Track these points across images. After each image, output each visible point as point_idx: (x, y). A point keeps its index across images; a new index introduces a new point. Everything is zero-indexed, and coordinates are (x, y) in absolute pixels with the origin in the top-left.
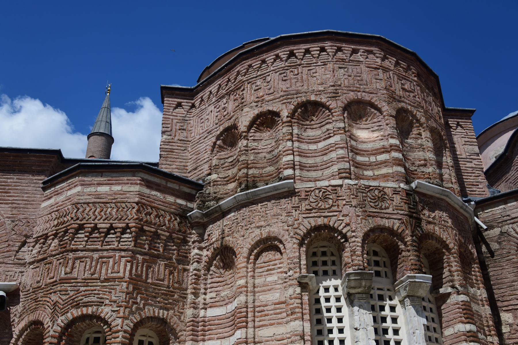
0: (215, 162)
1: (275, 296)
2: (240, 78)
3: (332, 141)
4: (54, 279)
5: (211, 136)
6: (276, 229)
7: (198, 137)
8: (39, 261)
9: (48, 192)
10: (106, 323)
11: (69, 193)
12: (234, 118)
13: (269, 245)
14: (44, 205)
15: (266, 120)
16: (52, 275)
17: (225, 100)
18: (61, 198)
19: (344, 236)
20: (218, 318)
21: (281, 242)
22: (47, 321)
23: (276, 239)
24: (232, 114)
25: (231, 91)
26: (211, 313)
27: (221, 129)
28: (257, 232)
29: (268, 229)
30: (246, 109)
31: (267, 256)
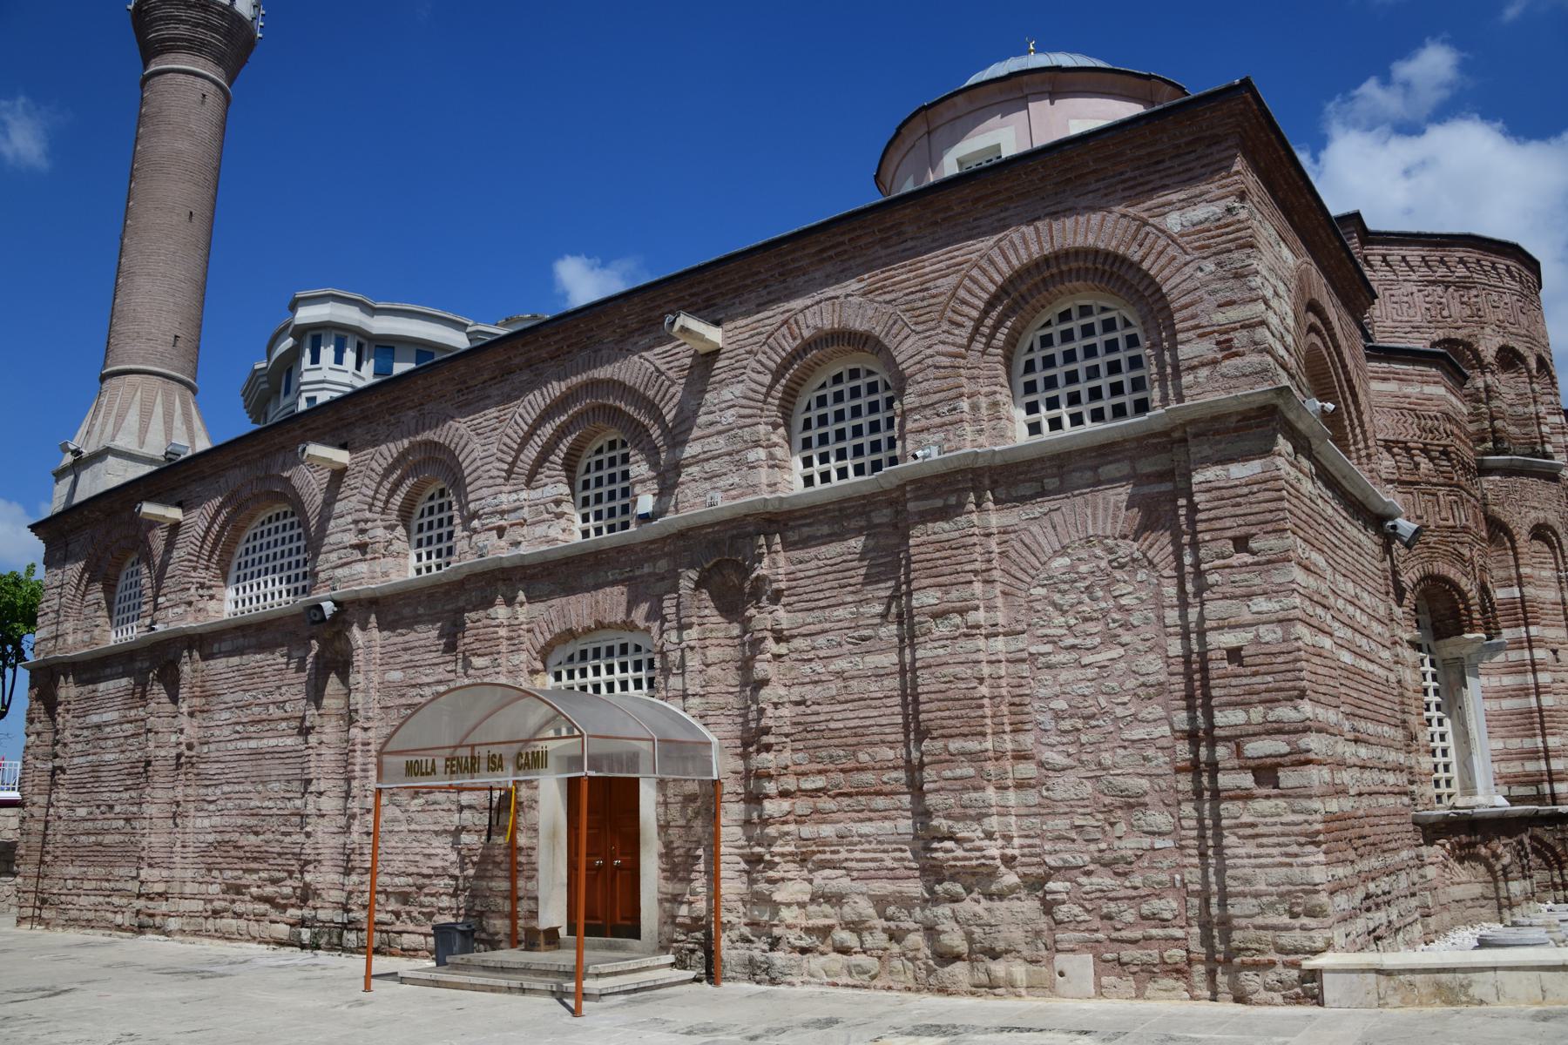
4: (1451, 523)
5: (1417, 335)
6: (1552, 518)
7: (1389, 323)
8: (1402, 483)
9: (1374, 365)
12: (1465, 331)
14: (1375, 386)
16: (1444, 514)
17: (1440, 290)
18: (1413, 390)
21: (1555, 533)
23: (1551, 528)
24: (1460, 323)
28: (1533, 514)
29: (1542, 515)
30: (1488, 330)
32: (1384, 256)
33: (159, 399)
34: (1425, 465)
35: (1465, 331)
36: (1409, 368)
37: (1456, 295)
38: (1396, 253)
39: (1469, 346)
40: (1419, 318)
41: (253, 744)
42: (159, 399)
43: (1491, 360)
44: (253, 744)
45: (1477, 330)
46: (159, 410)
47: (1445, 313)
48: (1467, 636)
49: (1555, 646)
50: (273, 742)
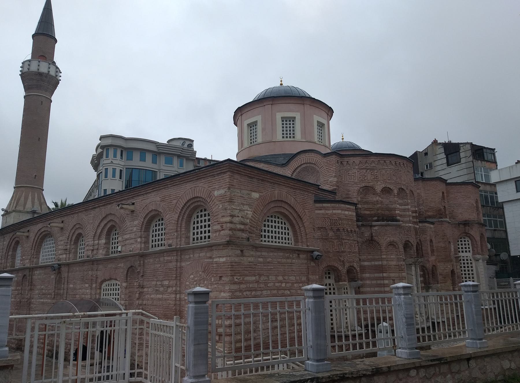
0: (359, 199)
1: (394, 263)
2: (373, 165)
3: (407, 207)
4: (338, 250)
10: (355, 268)
11: (334, 212)
12: (371, 184)
13: (392, 244)
15: (387, 191)
16: (335, 248)
17: (365, 171)
19: (412, 245)
20: (368, 266)
22: (340, 268)
25: (369, 169)
26: (366, 263)
27: (364, 185)
28: (389, 239)
31: (391, 248)
32: (347, 162)
33: (30, 194)
34: (331, 234)
35: (371, 184)
36: (329, 205)
37: (370, 172)
38: (351, 160)
39: (372, 187)
40: (357, 180)
41: (42, 300)
42: (30, 194)
43: (379, 192)
44: (42, 300)
45: (375, 183)
46: (30, 198)
47: (366, 178)
48: (341, 283)
49: (393, 279)
50: (47, 300)
